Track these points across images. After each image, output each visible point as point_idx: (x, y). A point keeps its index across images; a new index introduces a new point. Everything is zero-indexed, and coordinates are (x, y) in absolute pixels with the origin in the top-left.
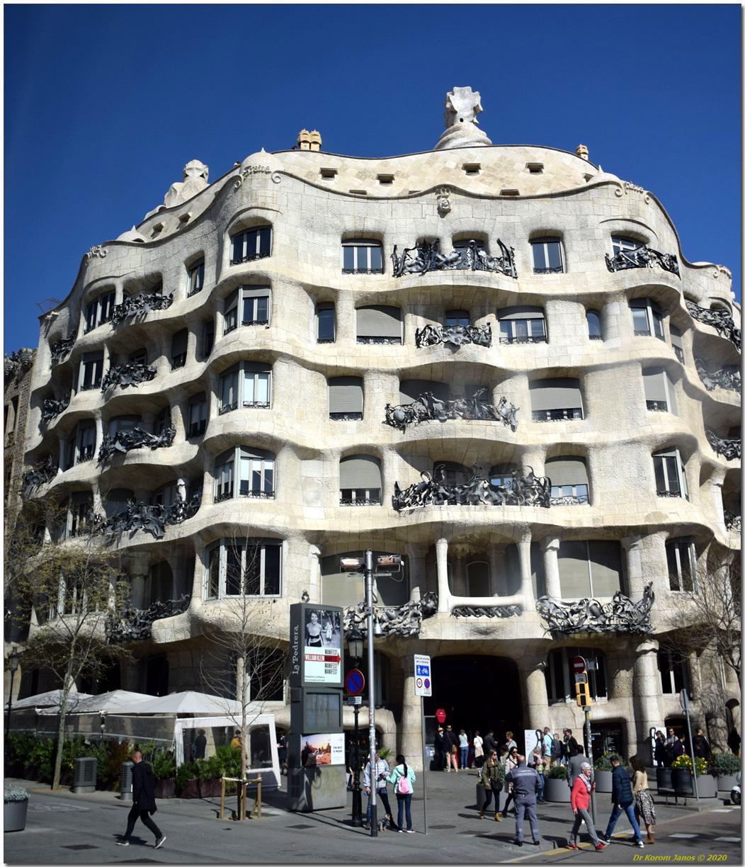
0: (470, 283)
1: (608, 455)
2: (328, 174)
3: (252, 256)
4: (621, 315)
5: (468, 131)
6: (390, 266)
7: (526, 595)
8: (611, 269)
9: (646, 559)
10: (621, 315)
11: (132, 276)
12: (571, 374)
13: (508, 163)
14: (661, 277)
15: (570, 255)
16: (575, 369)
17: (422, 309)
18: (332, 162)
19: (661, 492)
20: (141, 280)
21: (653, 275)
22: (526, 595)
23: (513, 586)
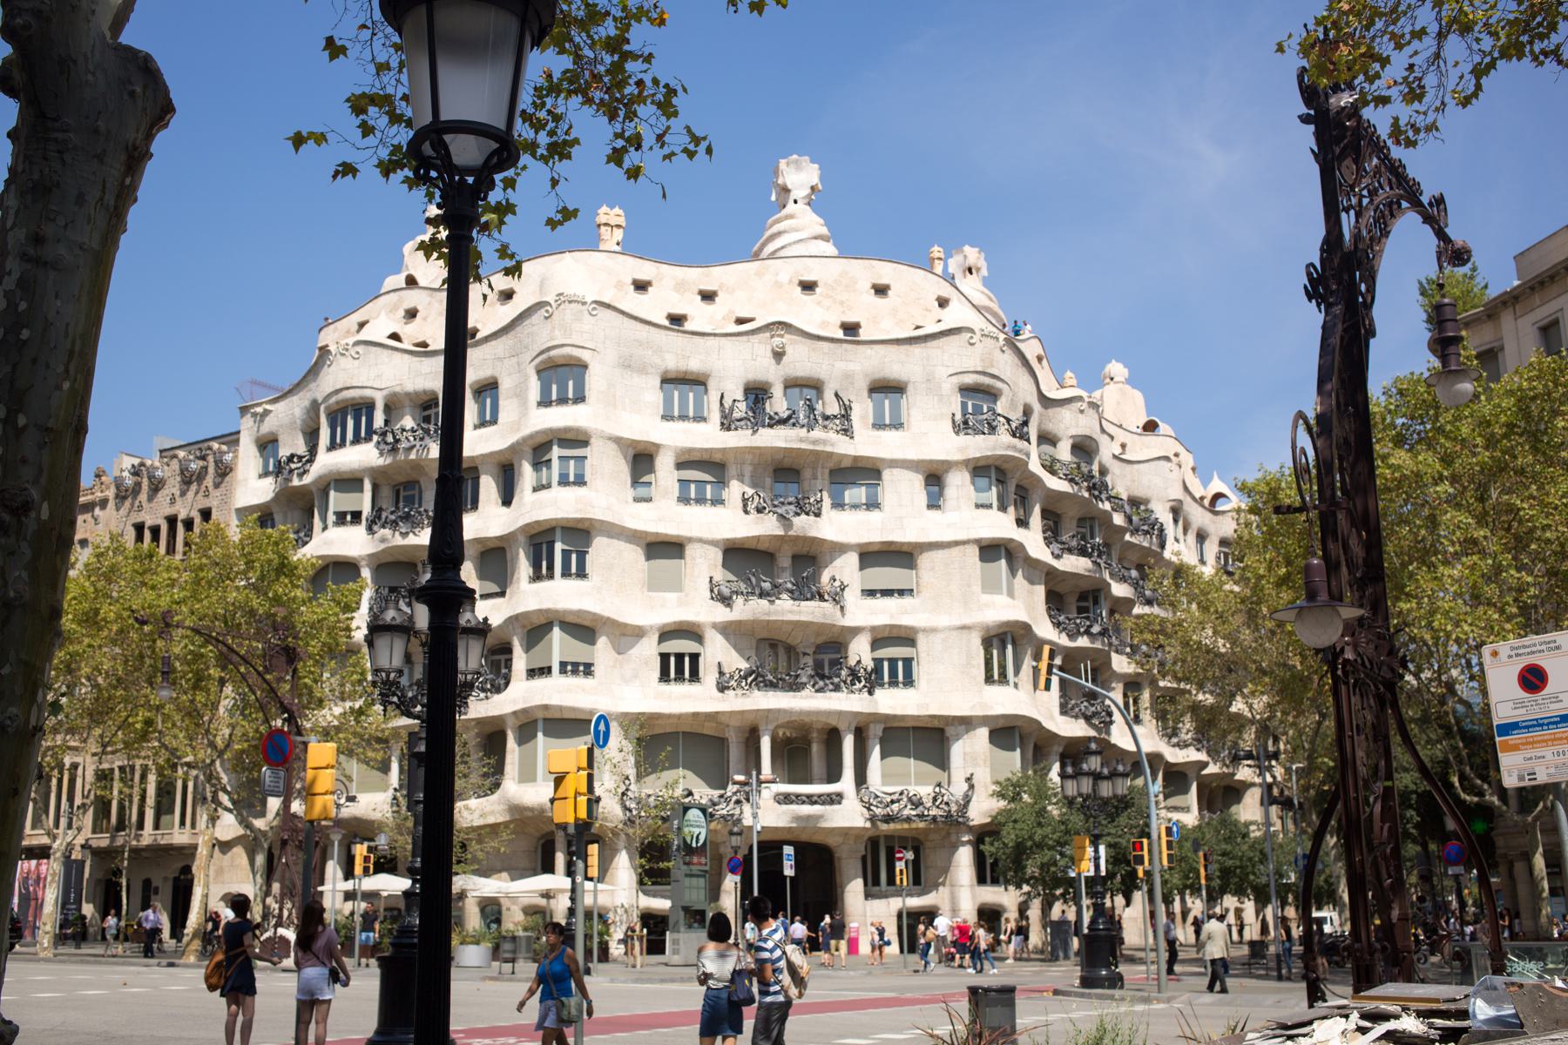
0: (804, 446)
1: (937, 639)
2: (641, 286)
3: (562, 401)
4: (959, 485)
5: (801, 224)
6: (715, 417)
7: (846, 784)
8: (957, 433)
9: (968, 750)
10: (959, 485)
11: (398, 389)
12: (904, 549)
13: (848, 285)
14: (1008, 447)
15: (913, 412)
16: (910, 544)
17: (748, 470)
18: (645, 269)
19: (989, 679)
20: (408, 394)
21: (999, 444)
22: (846, 784)
23: (834, 775)
